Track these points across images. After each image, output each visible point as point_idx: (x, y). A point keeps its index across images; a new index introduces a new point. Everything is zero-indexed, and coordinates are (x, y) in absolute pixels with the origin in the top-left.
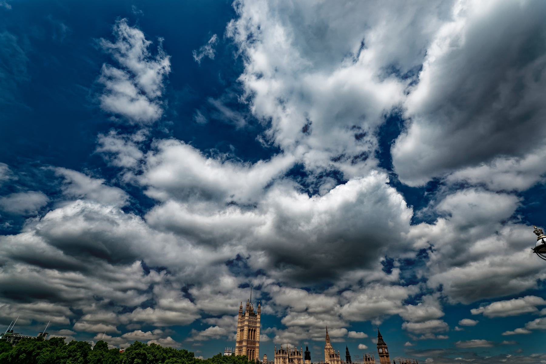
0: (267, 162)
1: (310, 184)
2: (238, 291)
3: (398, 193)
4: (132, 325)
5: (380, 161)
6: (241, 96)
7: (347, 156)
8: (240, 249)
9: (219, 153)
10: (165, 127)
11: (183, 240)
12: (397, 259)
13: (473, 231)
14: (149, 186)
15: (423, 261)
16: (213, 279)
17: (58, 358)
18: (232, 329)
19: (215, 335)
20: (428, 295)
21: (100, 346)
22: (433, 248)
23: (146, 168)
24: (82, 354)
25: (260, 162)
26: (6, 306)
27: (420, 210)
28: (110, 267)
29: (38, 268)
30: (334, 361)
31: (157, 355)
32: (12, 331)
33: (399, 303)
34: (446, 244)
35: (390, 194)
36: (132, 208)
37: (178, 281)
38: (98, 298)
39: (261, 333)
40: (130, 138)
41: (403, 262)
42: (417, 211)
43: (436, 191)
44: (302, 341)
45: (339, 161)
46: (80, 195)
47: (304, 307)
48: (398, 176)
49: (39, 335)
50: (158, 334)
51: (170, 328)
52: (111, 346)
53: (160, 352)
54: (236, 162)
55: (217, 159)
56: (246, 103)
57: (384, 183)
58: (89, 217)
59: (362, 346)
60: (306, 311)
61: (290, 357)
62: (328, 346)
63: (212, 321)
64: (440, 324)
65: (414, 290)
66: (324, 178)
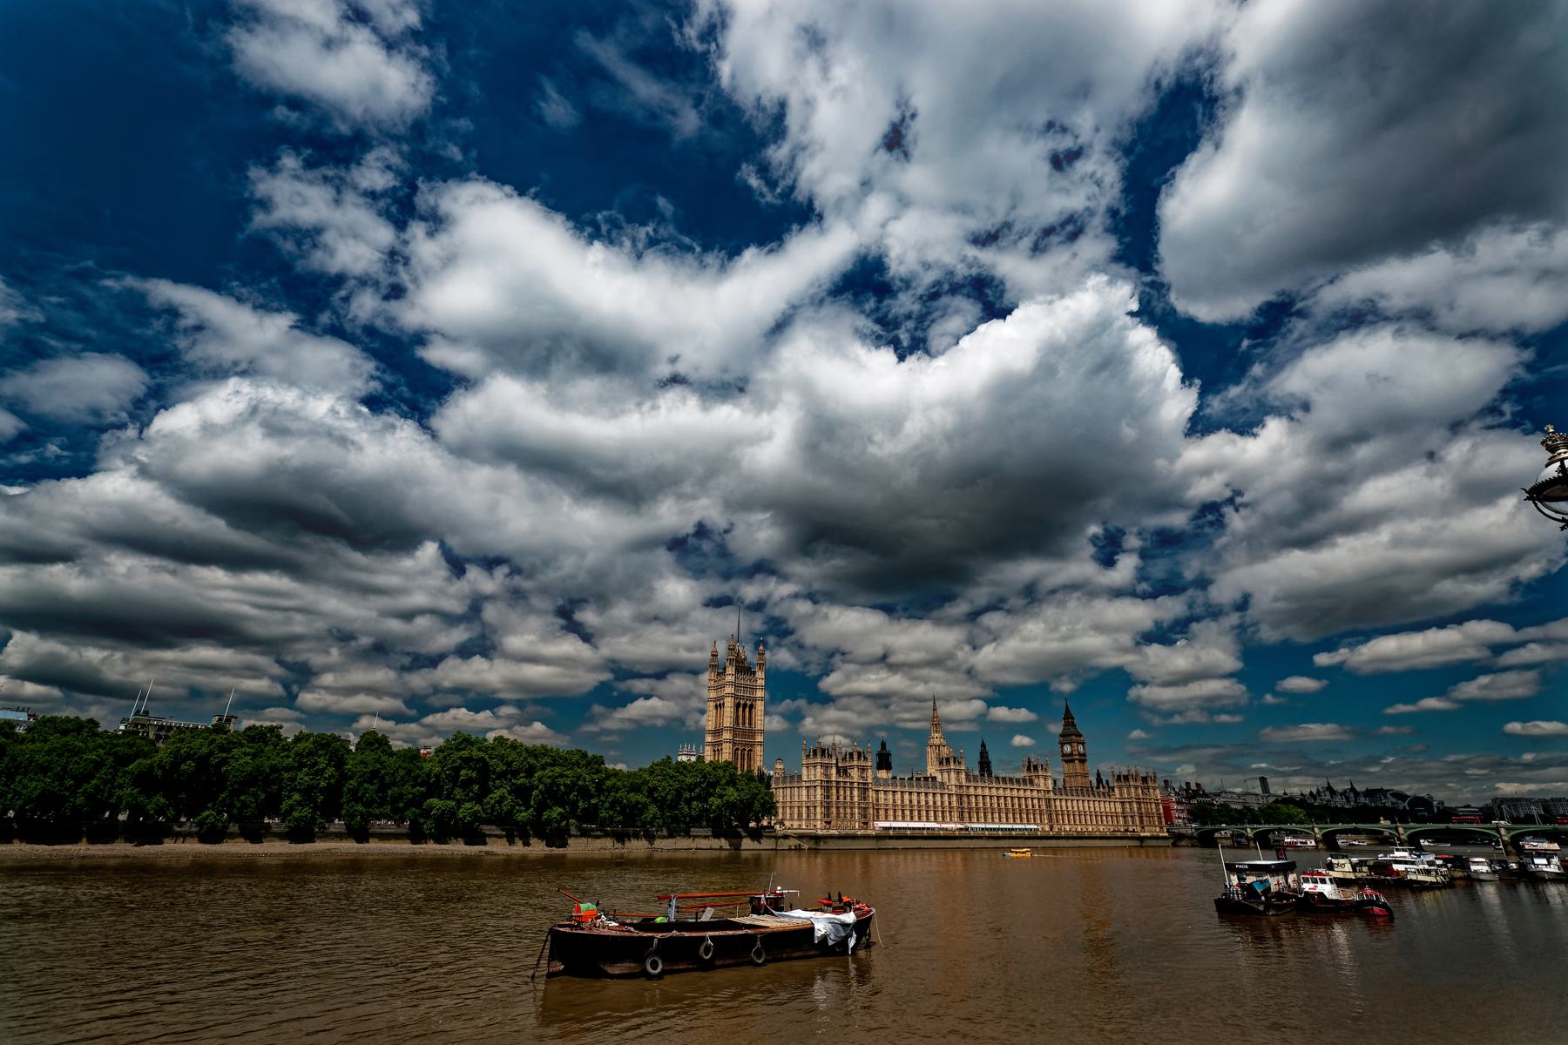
0: (771, 251)
1: (903, 318)
2: (705, 615)
3: (1162, 344)
4: (441, 695)
5: (1121, 243)
6: (685, 22)
7: (1017, 227)
8: (707, 509)
9: (624, 224)
10: (449, 141)
11: (544, 486)
12: (1135, 530)
13: (1364, 452)
14: (428, 333)
15: (1206, 535)
16: (637, 585)
17: (274, 769)
18: (694, 703)
19: (651, 717)
20: (1209, 619)
21: (371, 744)
22: (1239, 500)
23: (411, 275)
24: (330, 760)
25: (750, 254)
26: (111, 656)
27: (1218, 392)
28: (358, 557)
29: (171, 565)
30: (949, 771)
31: (512, 762)
32: (146, 713)
33: (1126, 639)
34: (1281, 488)
35: (1138, 347)
36: (390, 397)
37: (545, 591)
38: (344, 637)
39: (766, 713)
40: (348, 179)
41: (1149, 536)
42: (1210, 398)
43: (1275, 335)
44: (870, 730)
45: (994, 247)
46: (236, 363)
47: (878, 651)
48: (1169, 289)
49: (215, 720)
50: (509, 717)
51: (536, 702)
52: (399, 743)
53: (519, 754)
54: (678, 254)
55: (621, 245)
56: (699, 47)
57: (1121, 312)
58: (276, 426)
59: (1020, 740)
60: (884, 660)
61: (840, 765)
62: (937, 738)
63: (641, 685)
64: (1225, 688)
65: (1171, 608)
66: (944, 300)
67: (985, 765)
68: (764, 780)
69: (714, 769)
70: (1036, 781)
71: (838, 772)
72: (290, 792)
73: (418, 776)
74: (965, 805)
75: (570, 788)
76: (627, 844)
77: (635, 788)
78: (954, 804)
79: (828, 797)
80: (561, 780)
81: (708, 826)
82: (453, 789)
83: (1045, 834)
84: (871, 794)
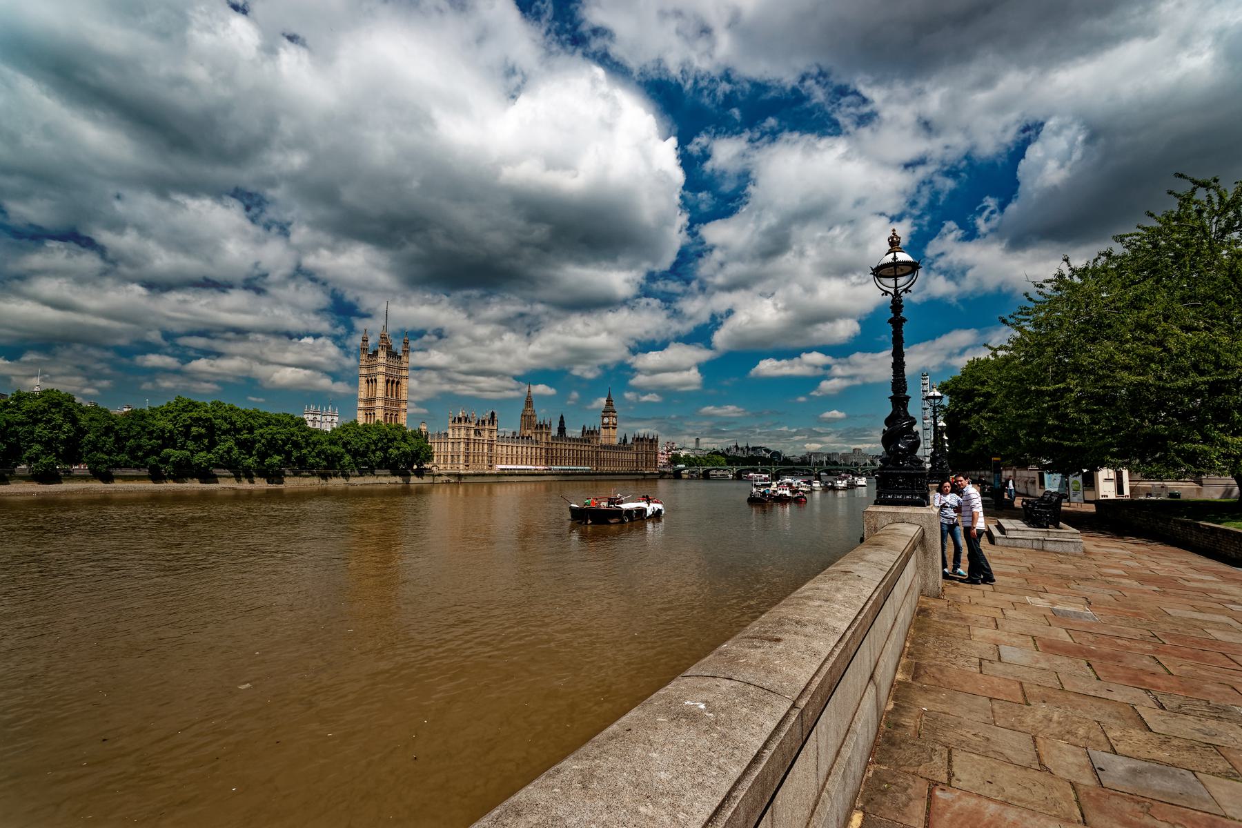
24: (65, 416)
31: (235, 422)
71: (475, 433)
72: (28, 442)
73: (153, 432)
74: (550, 455)
75: (285, 443)
76: (330, 481)
77: (333, 443)
78: (543, 454)
79: (468, 449)
80: (278, 436)
82: (185, 442)
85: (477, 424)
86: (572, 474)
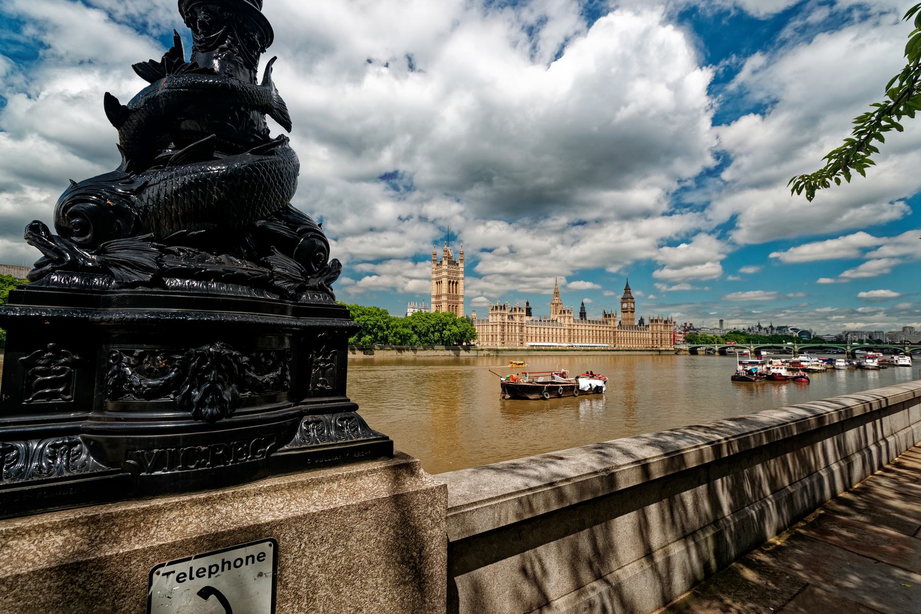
67: (583, 315)
68: (469, 321)
69: (445, 316)
70: (609, 322)
71: (509, 318)
75: (374, 326)
76: (403, 353)
77: (405, 326)
79: (503, 330)
80: (368, 322)
81: (443, 345)
83: (612, 349)
84: (525, 328)
85: (511, 311)
86: (591, 350)
